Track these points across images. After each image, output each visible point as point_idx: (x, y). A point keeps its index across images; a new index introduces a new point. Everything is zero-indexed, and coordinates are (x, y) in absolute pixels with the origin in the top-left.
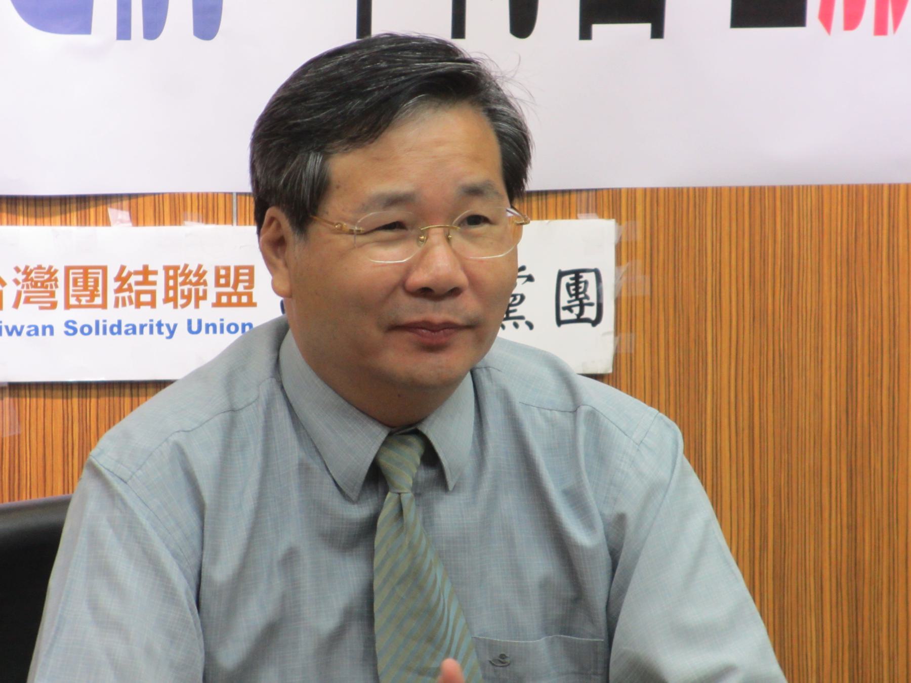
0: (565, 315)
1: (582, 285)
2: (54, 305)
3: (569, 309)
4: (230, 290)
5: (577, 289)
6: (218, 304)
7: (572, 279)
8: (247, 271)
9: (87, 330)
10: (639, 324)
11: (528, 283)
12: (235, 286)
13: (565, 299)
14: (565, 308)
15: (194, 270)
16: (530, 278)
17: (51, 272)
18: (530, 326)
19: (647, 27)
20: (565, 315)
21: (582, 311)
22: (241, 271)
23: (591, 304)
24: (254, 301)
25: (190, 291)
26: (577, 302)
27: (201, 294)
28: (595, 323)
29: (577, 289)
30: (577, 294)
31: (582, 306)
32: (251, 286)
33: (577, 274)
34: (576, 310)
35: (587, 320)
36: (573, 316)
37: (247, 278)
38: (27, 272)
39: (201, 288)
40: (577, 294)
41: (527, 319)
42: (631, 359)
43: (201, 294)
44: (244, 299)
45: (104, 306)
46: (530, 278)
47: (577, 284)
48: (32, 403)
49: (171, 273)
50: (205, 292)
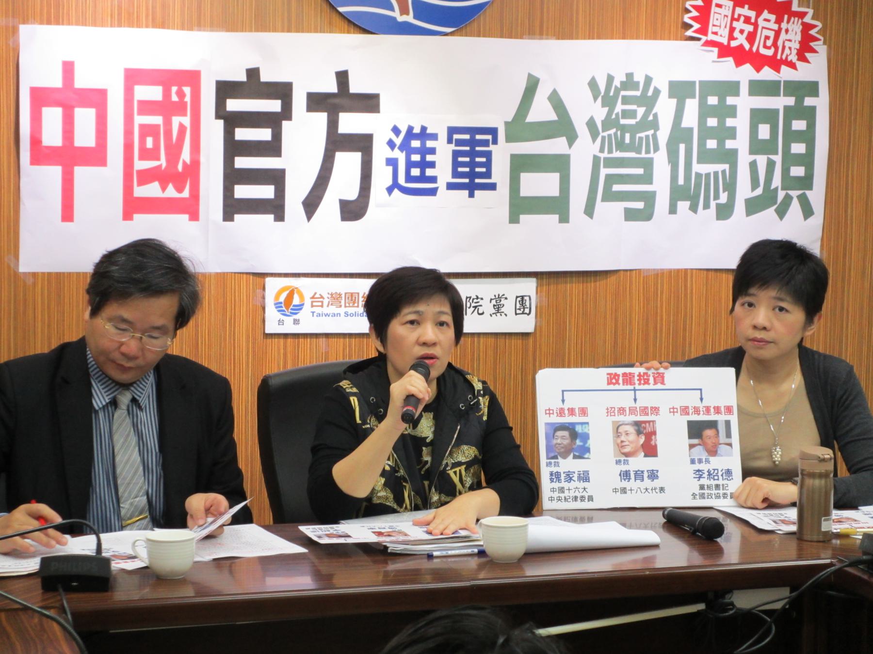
0: (518, 312)
2: (341, 306)
9: (352, 315)
13: (518, 306)
16: (506, 298)
17: (340, 295)
19: (556, 217)
20: (518, 312)
33: (522, 297)
38: (332, 294)
42: (541, 327)
45: (358, 306)
46: (506, 298)
48: (334, 340)
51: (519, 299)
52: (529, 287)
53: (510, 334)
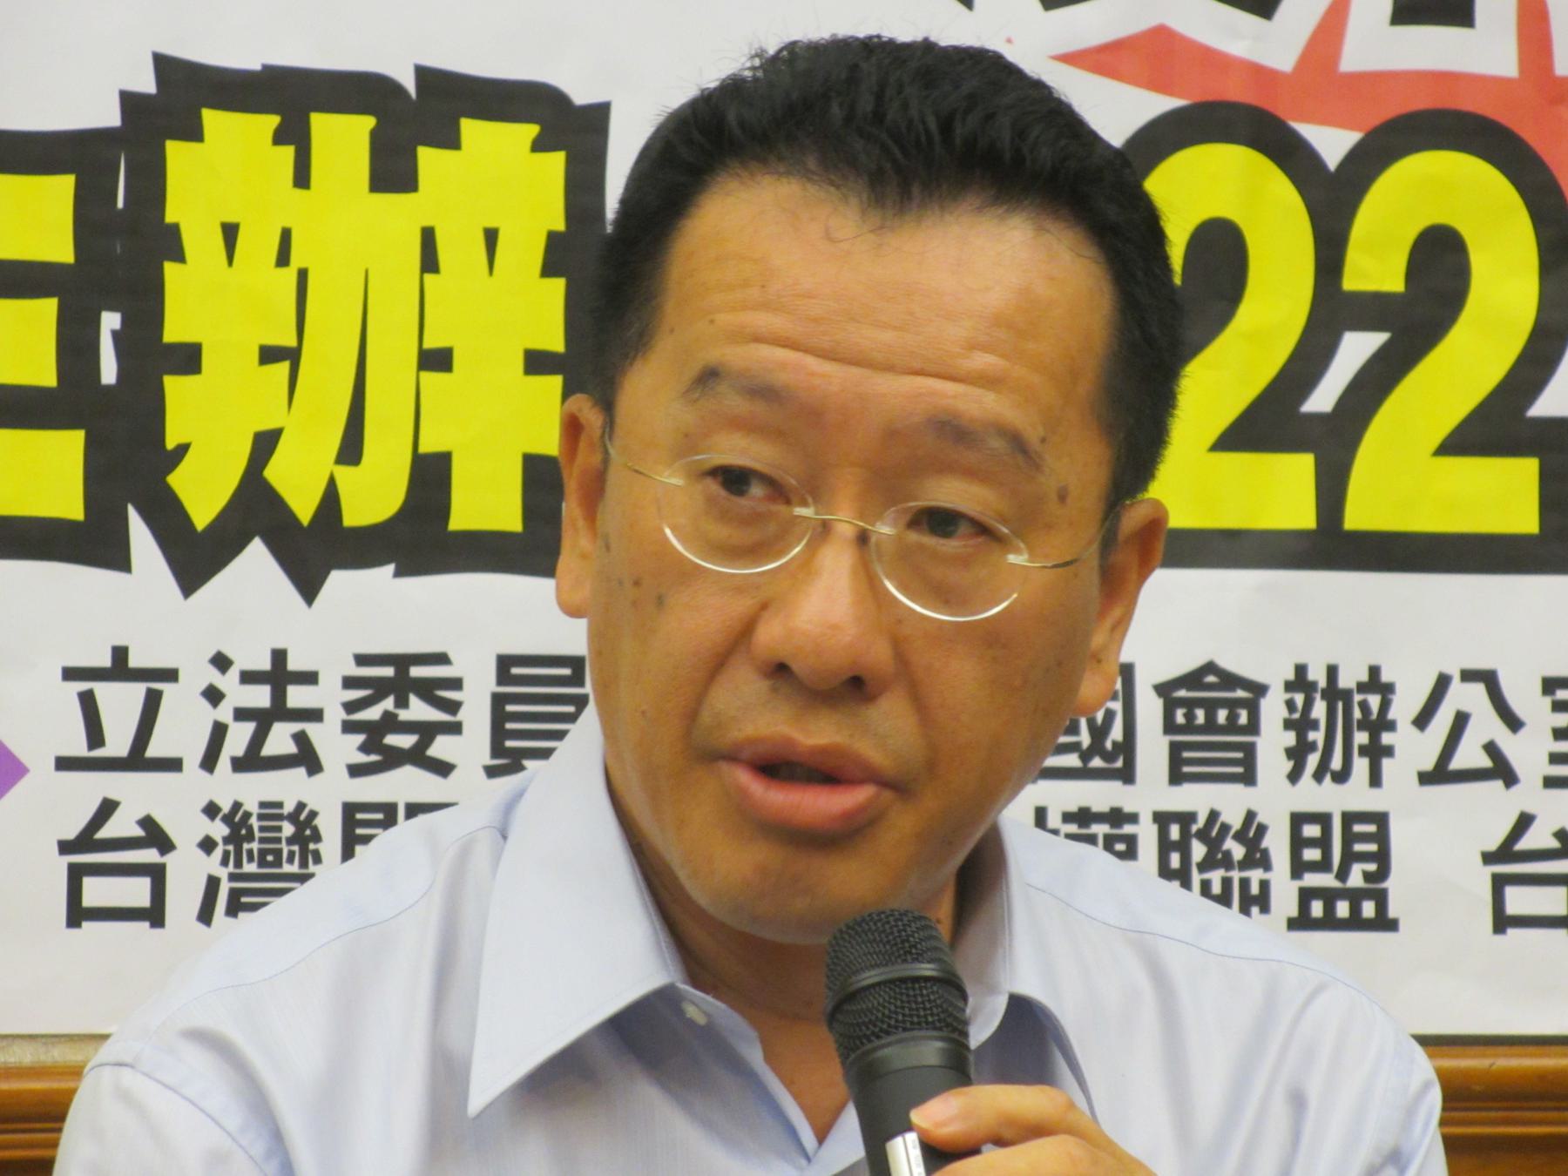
4: (1326, 880)
6: (1302, 922)
8: (1372, 828)
12: (1343, 875)
15: (1236, 823)
22: (1358, 828)
24: (1392, 914)
25: (1226, 883)
27: (1255, 889)
32: (1383, 872)
37: (1373, 847)
39: (1256, 875)
43: (1255, 889)
44: (1368, 909)
49: (1175, 832)
50: (1265, 885)
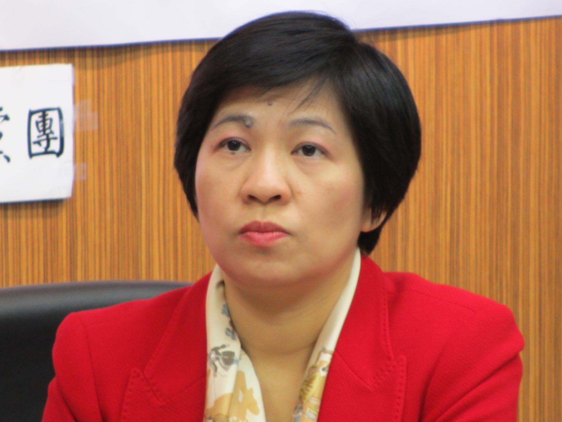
0: (36, 149)
1: (48, 122)
3: (39, 143)
5: (44, 125)
7: (40, 117)
10: (90, 154)
11: (6, 122)
13: (35, 134)
14: (35, 143)
18: (8, 159)
20: (36, 149)
21: (48, 145)
23: (55, 138)
26: (45, 137)
28: (59, 154)
29: (44, 125)
30: (44, 130)
31: (48, 140)
33: (44, 112)
34: (44, 144)
35: (52, 152)
36: (41, 149)
40: (44, 130)
41: (6, 153)
42: (84, 184)
46: (6, 118)
47: (44, 121)
51: (36, 118)
52: (55, 85)
53: (17, 206)
